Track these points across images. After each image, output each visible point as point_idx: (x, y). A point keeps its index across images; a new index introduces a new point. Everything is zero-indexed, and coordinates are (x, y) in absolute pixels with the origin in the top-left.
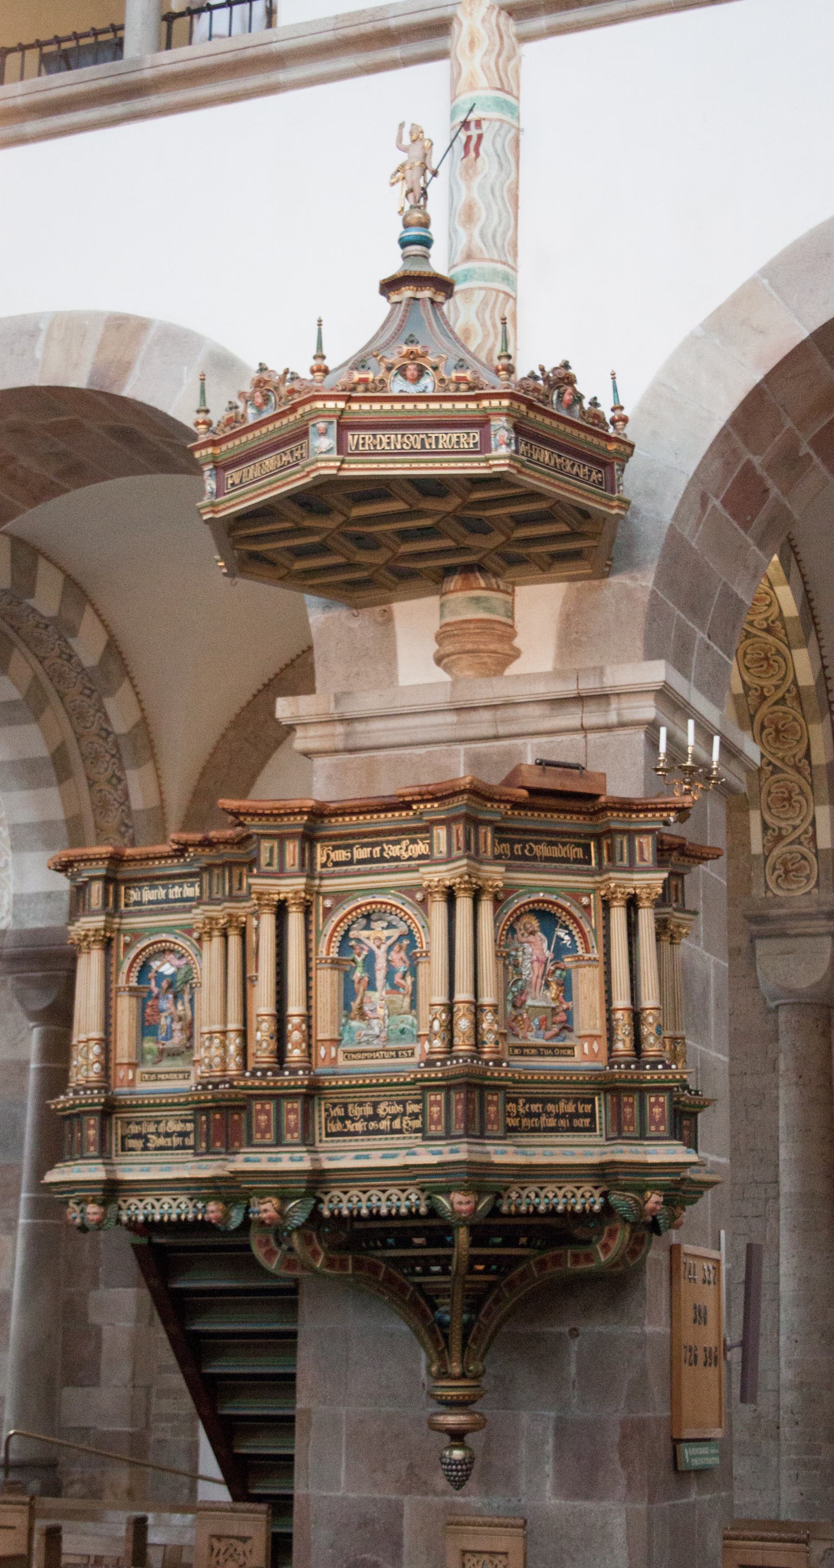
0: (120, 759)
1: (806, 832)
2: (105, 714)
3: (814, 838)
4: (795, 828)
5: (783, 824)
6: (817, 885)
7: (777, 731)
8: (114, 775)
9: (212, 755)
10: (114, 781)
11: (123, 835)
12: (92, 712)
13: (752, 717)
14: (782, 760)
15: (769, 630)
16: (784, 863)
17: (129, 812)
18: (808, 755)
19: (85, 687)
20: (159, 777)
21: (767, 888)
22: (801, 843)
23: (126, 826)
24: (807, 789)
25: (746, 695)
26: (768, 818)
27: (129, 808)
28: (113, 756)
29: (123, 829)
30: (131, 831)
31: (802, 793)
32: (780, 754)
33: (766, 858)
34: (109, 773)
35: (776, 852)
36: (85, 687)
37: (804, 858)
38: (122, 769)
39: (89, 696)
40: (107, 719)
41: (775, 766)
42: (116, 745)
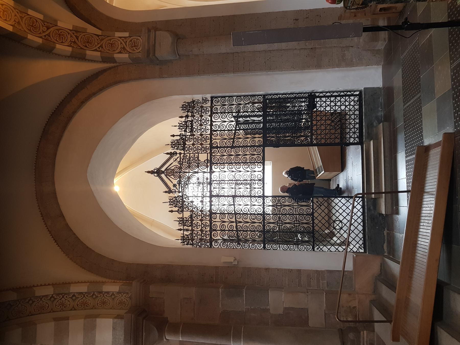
0: (65, 294)
1: (123, 40)
2: (43, 296)
3: (125, 38)
4: (121, 43)
5: (120, 47)
6: (140, 36)
7: (88, 42)
8: (72, 298)
9: (77, 264)
10: (74, 298)
11: (97, 297)
12: (41, 302)
13: (81, 48)
14: (98, 44)
15: (48, 28)
16: (132, 47)
17: (88, 293)
18: (98, 36)
19: (28, 302)
20: (78, 282)
21: (139, 52)
22: (126, 42)
23: (93, 295)
24: (109, 38)
25: (73, 47)
26: (117, 52)
27: (86, 293)
28: (63, 297)
29: (94, 296)
30: (95, 293)
31: (110, 40)
32: (96, 44)
33: (130, 52)
34: (70, 300)
35: (128, 50)
36: (28, 302)
37: (131, 41)
38: (69, 294)
39: (33, 302)
40: (47, 296)
41: (100, 46)
42: (58, 295)
